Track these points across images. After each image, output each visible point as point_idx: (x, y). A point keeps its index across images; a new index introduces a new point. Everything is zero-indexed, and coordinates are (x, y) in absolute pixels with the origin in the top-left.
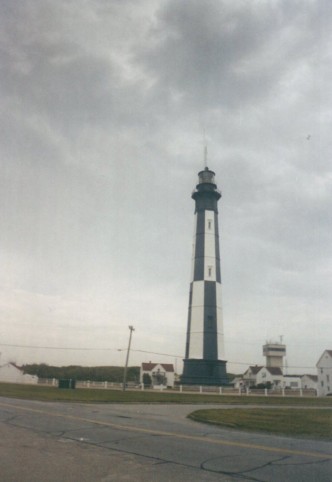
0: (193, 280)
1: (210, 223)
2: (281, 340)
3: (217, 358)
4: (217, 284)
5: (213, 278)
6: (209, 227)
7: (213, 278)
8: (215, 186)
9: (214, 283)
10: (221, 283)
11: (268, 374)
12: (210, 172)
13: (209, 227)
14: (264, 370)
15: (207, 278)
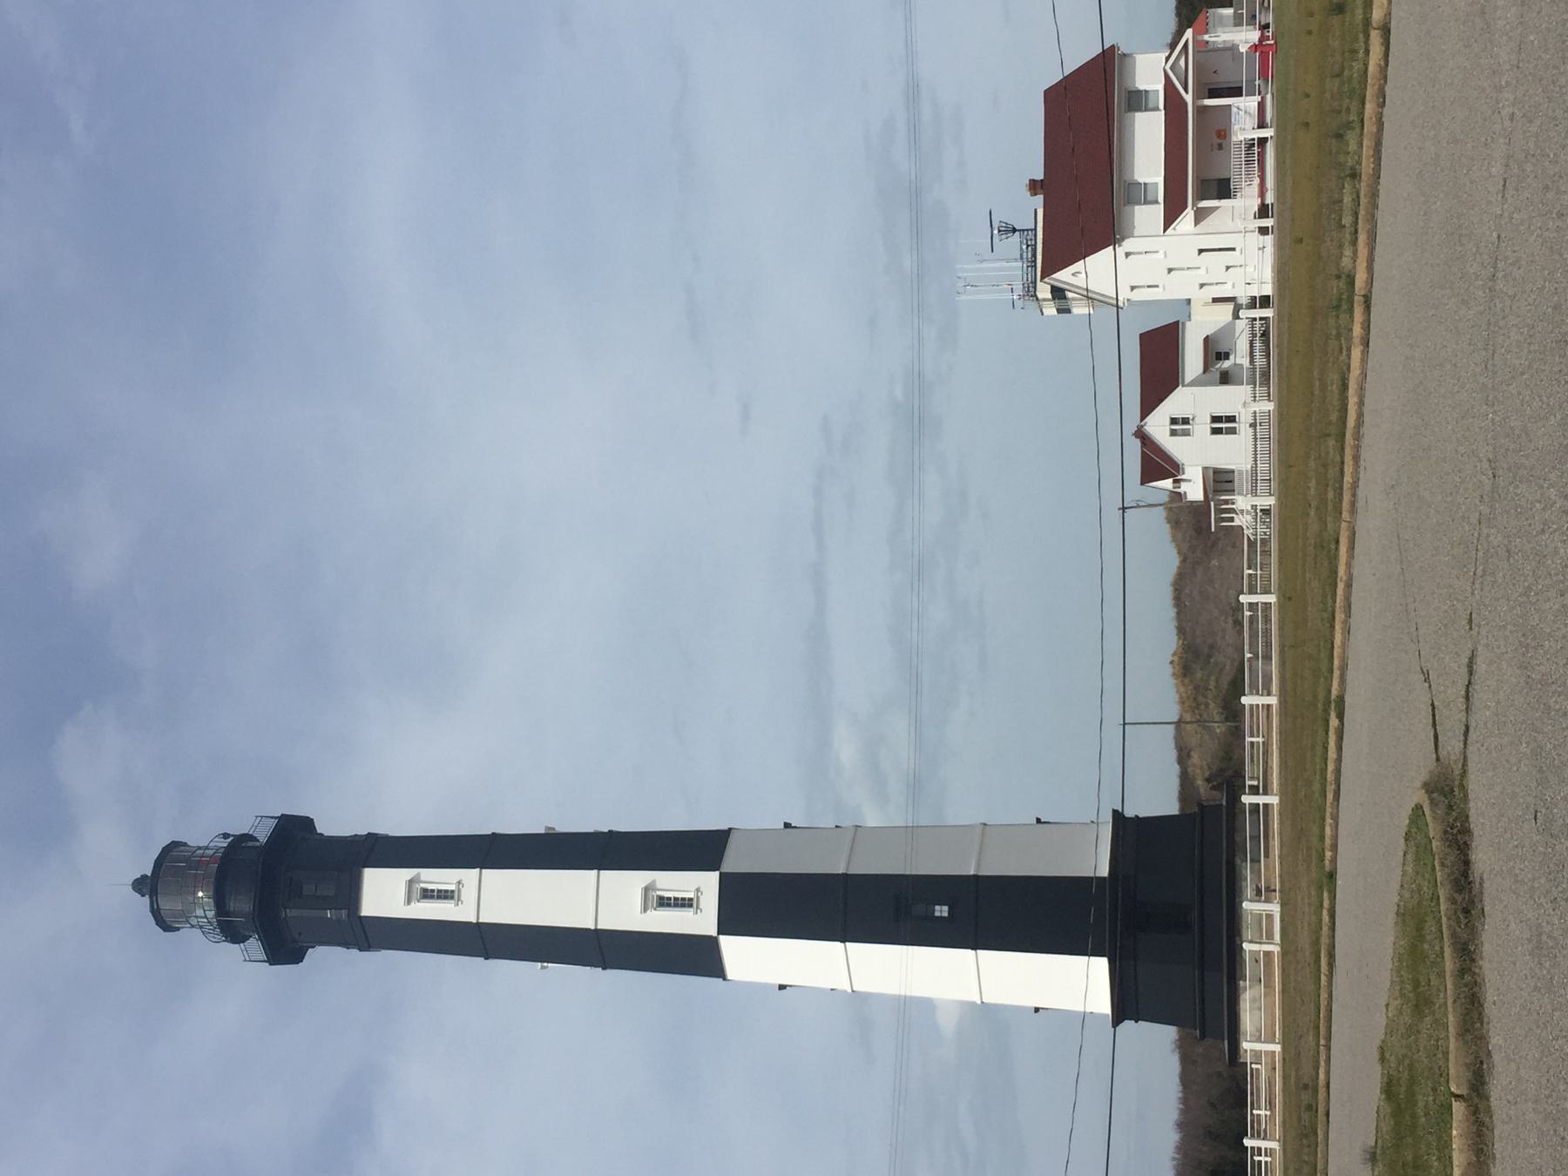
0: (721, 979)
1: (427, 895)
2: (1014, 230)
3: (1105, 878)
4: (734, 861)
5: (704, 885)
6: (445, 895)
7: (704, 885)
8: (239, 843)
9: (724, 879)
10: (730, 829)
11: (1178, 402)
12: (159, 863)
13: (445, 895)
14: (1157, 425)
15: (703, 922)
